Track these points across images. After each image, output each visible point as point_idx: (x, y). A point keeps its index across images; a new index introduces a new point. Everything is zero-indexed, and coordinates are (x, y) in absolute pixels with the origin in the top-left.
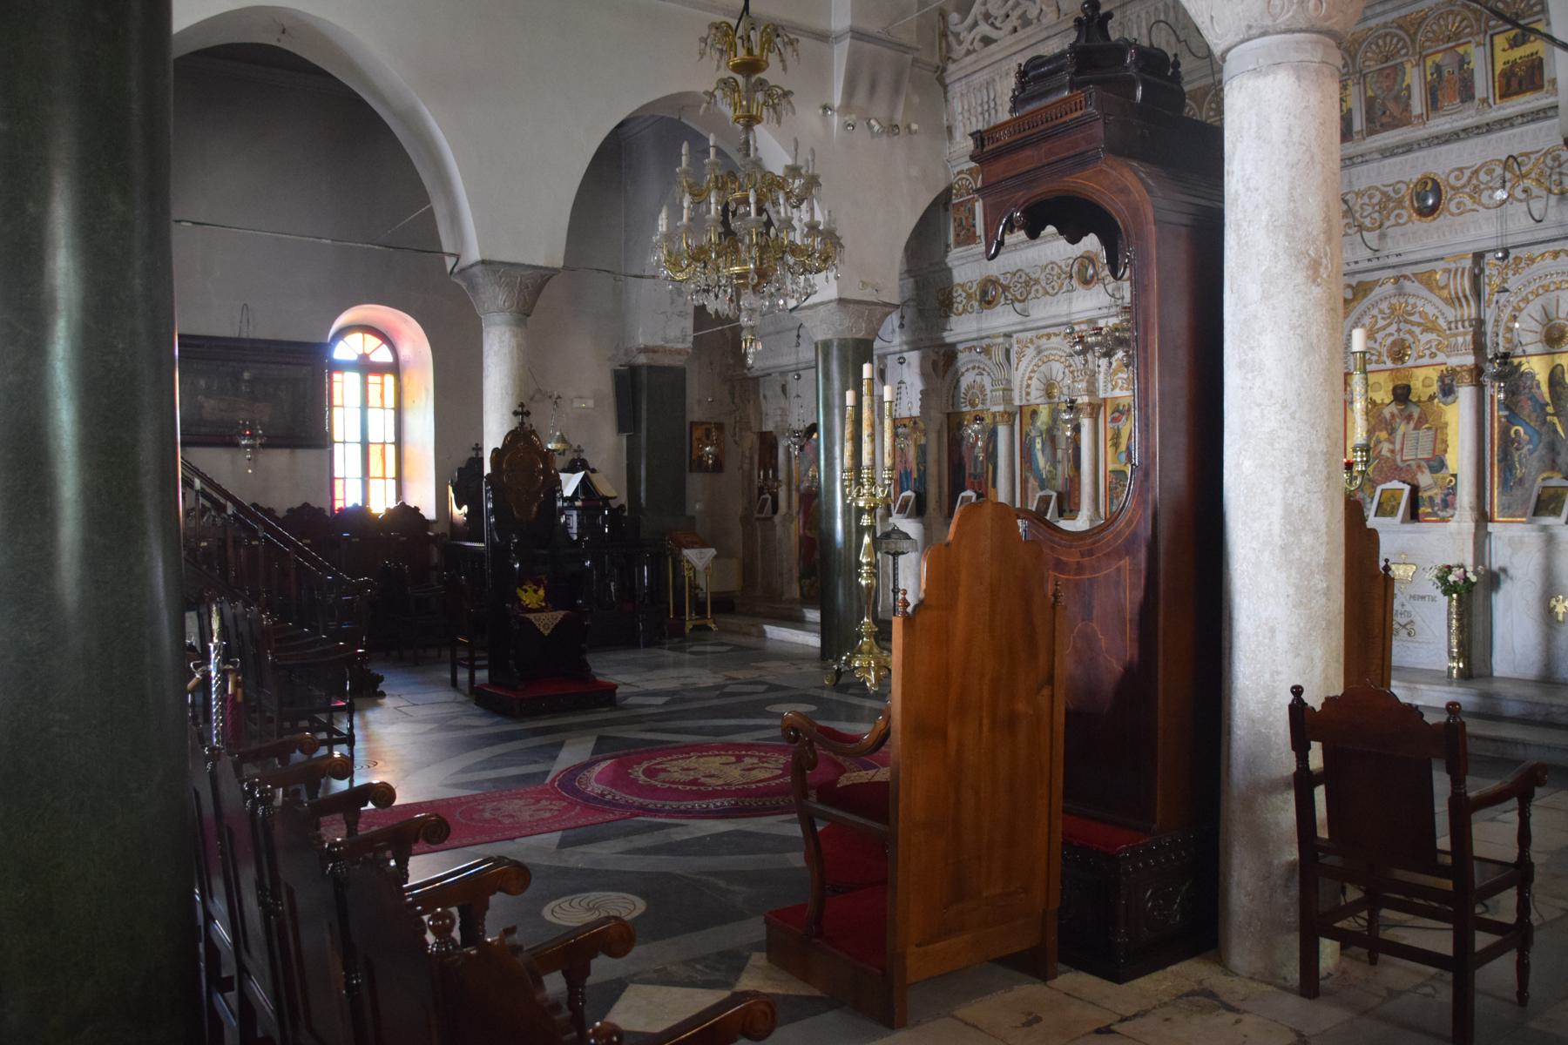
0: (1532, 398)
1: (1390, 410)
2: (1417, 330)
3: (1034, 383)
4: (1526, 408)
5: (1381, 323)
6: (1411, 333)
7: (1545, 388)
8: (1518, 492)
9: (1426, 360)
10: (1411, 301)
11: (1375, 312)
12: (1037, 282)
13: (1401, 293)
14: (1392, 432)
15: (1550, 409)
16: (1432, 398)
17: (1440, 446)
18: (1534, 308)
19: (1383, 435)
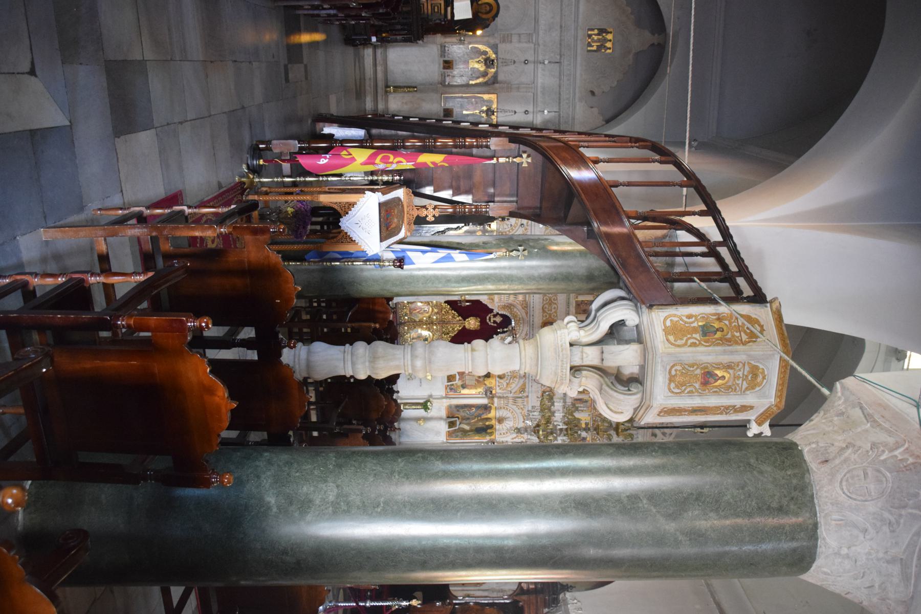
0: (483, 414)
2: (508, 381)
4: (480, 412)
6: (507, 379)
7: (486, 417)
8: (455, 410)
9: (497, 384)
10: (517, 380)
15: (479, 418)
16: (485, 384)
17: (469, 387)
18: (509, 415)
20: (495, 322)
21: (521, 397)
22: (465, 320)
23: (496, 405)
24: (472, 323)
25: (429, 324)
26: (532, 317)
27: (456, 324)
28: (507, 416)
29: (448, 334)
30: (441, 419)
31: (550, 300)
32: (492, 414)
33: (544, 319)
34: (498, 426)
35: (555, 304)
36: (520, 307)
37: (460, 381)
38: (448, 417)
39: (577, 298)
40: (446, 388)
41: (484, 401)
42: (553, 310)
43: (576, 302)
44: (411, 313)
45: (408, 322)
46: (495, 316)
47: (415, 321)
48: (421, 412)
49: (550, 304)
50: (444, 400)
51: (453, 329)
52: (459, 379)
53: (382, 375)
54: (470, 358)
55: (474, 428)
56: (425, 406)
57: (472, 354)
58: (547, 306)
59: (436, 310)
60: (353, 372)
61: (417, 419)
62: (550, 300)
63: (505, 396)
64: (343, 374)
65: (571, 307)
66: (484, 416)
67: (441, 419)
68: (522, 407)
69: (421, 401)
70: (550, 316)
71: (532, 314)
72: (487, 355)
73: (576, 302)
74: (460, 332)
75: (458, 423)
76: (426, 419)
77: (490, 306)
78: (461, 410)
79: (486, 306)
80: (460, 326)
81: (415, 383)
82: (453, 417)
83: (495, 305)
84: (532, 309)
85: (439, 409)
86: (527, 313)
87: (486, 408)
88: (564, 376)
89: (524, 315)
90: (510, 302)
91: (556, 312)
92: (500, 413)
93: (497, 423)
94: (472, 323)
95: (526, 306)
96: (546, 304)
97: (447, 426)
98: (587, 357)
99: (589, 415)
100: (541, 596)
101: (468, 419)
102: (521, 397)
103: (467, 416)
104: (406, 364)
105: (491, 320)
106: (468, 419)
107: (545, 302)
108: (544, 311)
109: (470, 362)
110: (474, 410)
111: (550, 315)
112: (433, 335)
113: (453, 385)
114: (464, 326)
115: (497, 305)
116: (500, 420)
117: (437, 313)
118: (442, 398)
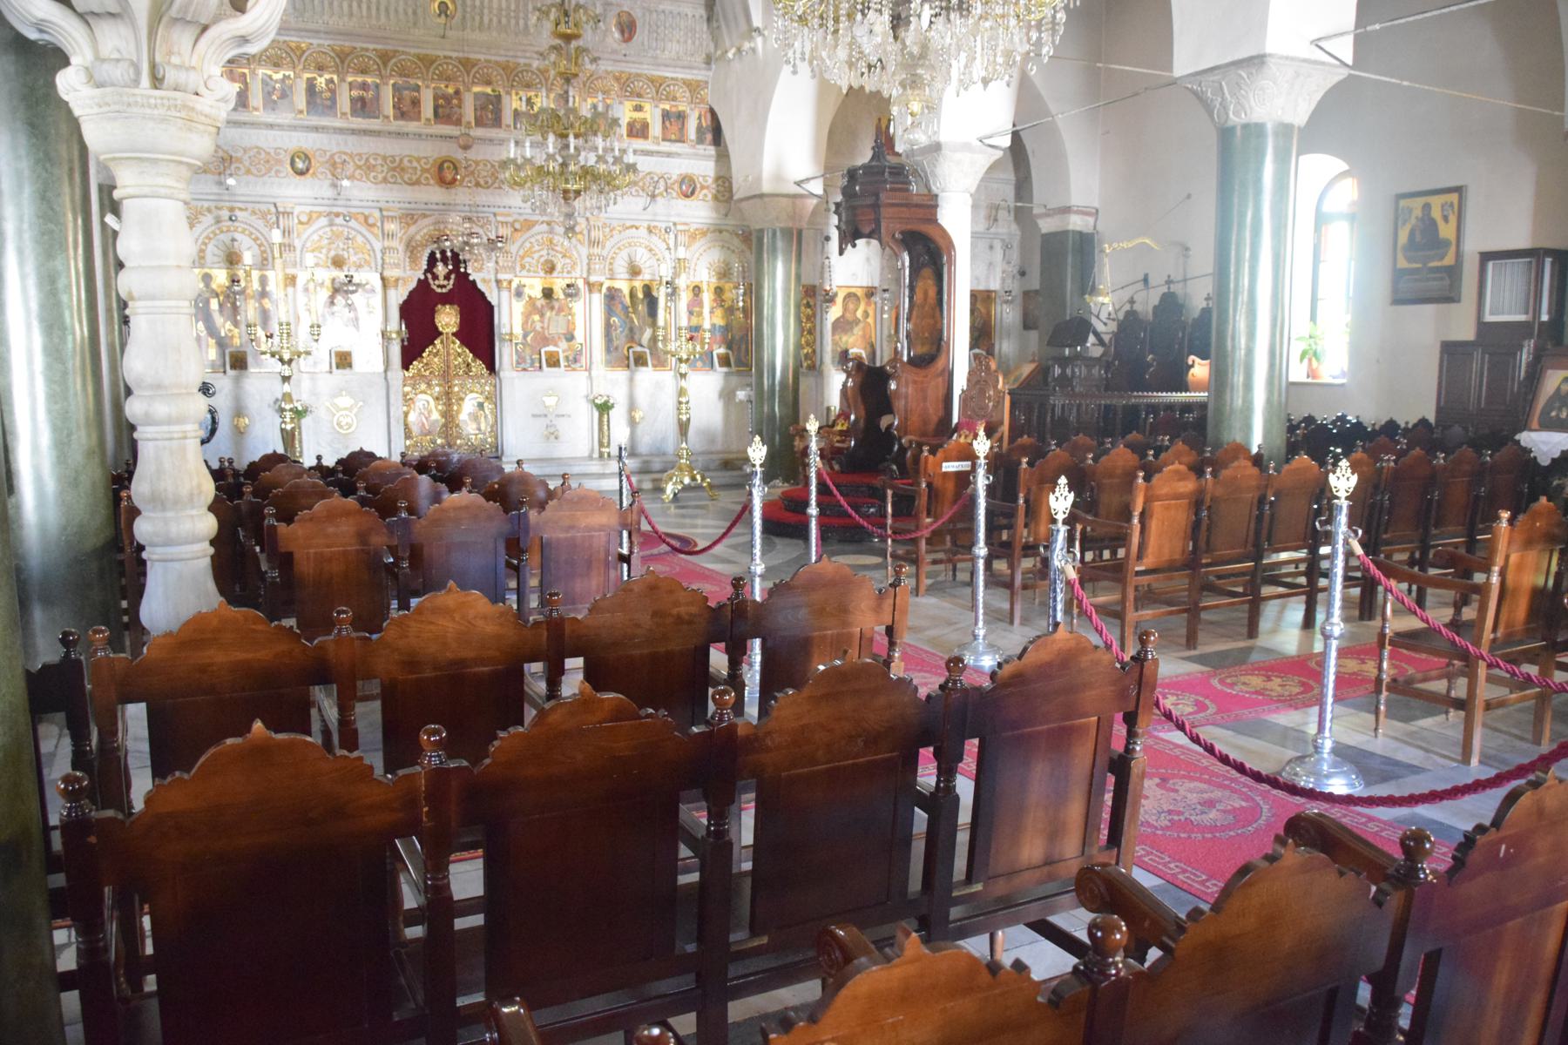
0: (622, 303)
1: (541, 302)
3: (211, 248)
5: (537, 248)
7: (628, 299)
11: (533, 240)
12: (239, 160)
13: (551, 231)
14: (542, 315)
17: (571, 327)
18: (624, 254)
19: (537, 318)
20: (447, 277)
21: (589, 232)
22: (441, 334)
23: (602, 279)
24: (448, 319)
25: (449, 399)
26: (430, 206)
27: (448, 349)
28: (627, 258)
29: (468, 365)
30: (631, 380)
31: (394, 169)
32: (624, 287)
33: (432, 182)
34: (646, 277)
35: (401, 160)
36: (413, 229)
37: (560, 344)
38: (628, 366)
39: (387, 117)
40: (574, 370)
41: (598, 300)
42: (415, 164)
43: (396, 118)
44: (429, 433)
45: (446, 437)
46: (435, 277)
47: (445, 425)
48: (618, 417)
49: (403, 170)
50: (594, 373)
51: (459, 355)
52: (556, 345)
53: (209, 488)
54: (149, 303)
55: (649, 320)
56: (604, 408)
57: (139, 299)
58: (406, 177)
59: (423, 386)
60: (200, 541)
61: (633, 423)
62: (394, 169)
63: (585, 261)
64: (208, 561)
65: (406, 130)
66: (628, 300)
67: (631, 380)
68: (607, 230)
69: (596, 414)
70: (427, 171)
71: (424, 206)
72: (140, 267)
73: (396, 118)
74: (464, 342)
75: (639, 349)
76: (632, 407)
77: (413, 285)
78: (616, 343)
79: (411, 293)
80: (454, 343)
81: (562, 425)
82: (628, 358)
83: (409, 277)
84: (412, 206)
85: (612, 383)
86: (425, 216)
87: (612, 296)
88: (165, 101)
89: (427, 221)
90: (401, 248)
91: (418, 160)
92: (621, 268)
93: (640, 277)
94: (448, 319)
95: (409, 218)
96: (402, 178)
97: (643, 369)
98: (119, 51)
99: (621, 103)
100: (883, 196)
101: (631, 330)
102: (589, 232)
103: (626, 331)
104: (168, 436)
105: (443, 282)
106: (631, 330)
107: (399, 180)
108: (417, 183)
109: (157, 303)
110: (614, 319)
111: (424, 171)
112: (472, 392)
113: (567, 358)
114: (454, 334)
115: (409, 273)
116: (634, 271)
117: (429, 385)
118: (590, 377)
